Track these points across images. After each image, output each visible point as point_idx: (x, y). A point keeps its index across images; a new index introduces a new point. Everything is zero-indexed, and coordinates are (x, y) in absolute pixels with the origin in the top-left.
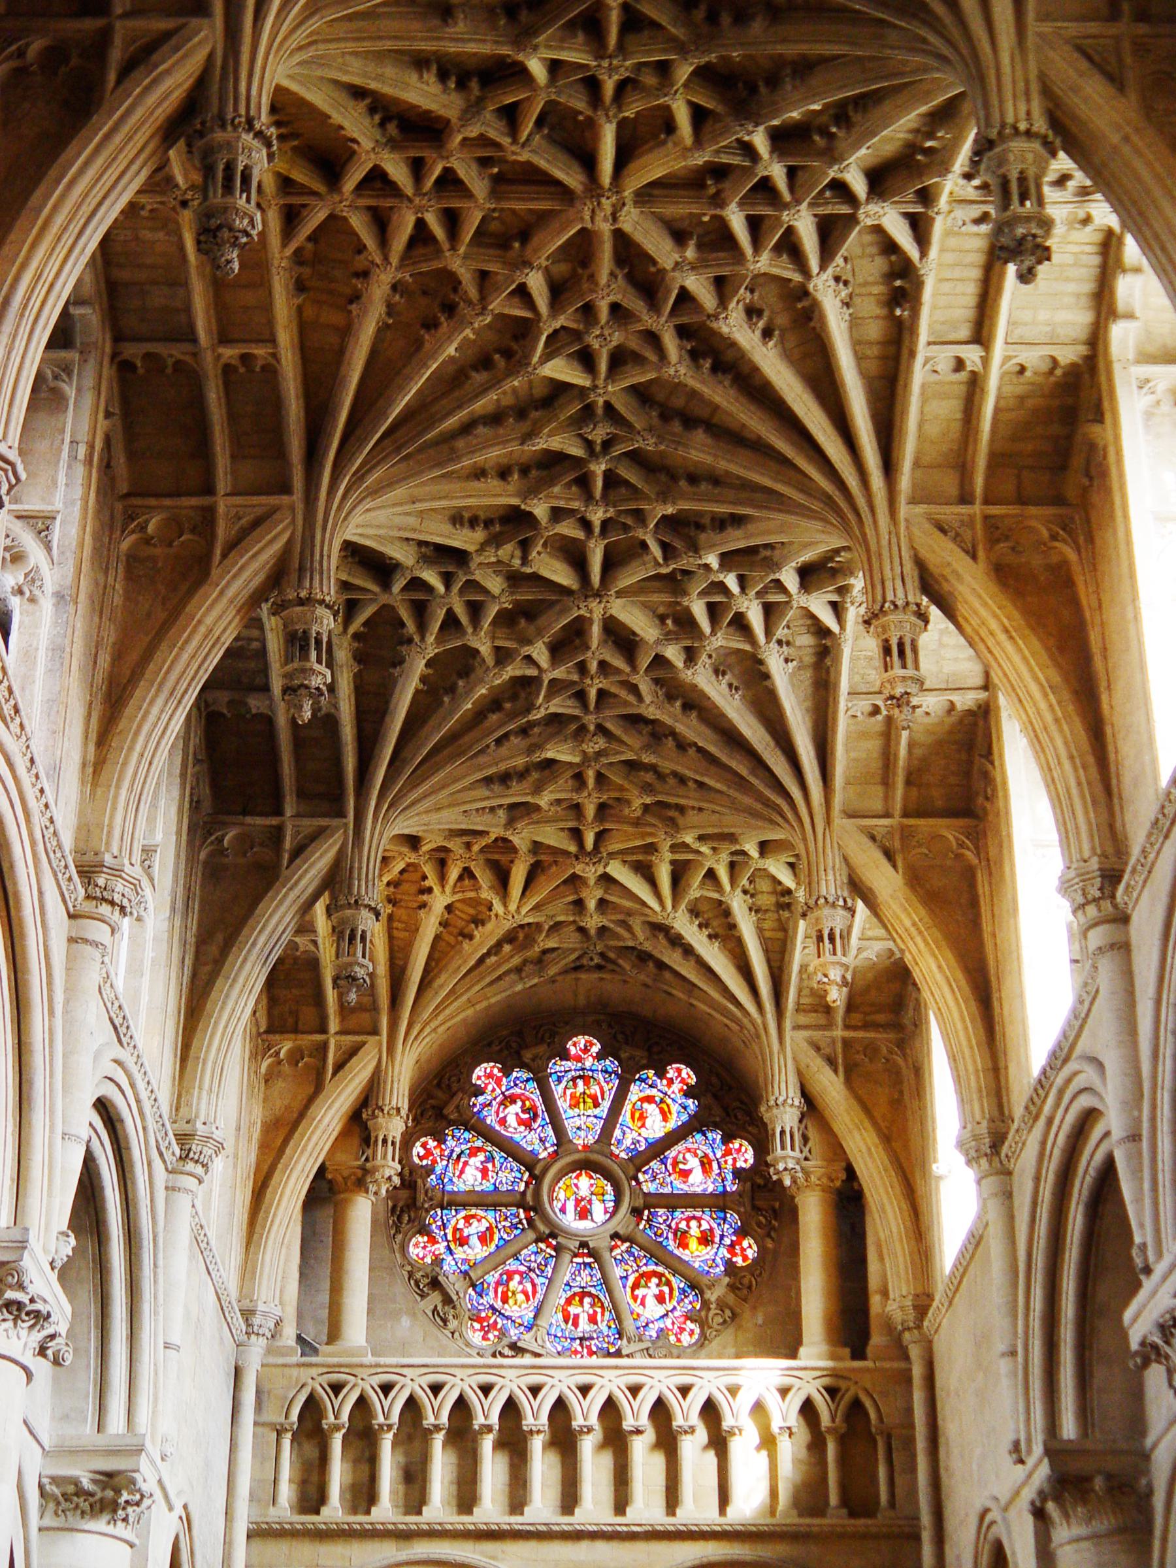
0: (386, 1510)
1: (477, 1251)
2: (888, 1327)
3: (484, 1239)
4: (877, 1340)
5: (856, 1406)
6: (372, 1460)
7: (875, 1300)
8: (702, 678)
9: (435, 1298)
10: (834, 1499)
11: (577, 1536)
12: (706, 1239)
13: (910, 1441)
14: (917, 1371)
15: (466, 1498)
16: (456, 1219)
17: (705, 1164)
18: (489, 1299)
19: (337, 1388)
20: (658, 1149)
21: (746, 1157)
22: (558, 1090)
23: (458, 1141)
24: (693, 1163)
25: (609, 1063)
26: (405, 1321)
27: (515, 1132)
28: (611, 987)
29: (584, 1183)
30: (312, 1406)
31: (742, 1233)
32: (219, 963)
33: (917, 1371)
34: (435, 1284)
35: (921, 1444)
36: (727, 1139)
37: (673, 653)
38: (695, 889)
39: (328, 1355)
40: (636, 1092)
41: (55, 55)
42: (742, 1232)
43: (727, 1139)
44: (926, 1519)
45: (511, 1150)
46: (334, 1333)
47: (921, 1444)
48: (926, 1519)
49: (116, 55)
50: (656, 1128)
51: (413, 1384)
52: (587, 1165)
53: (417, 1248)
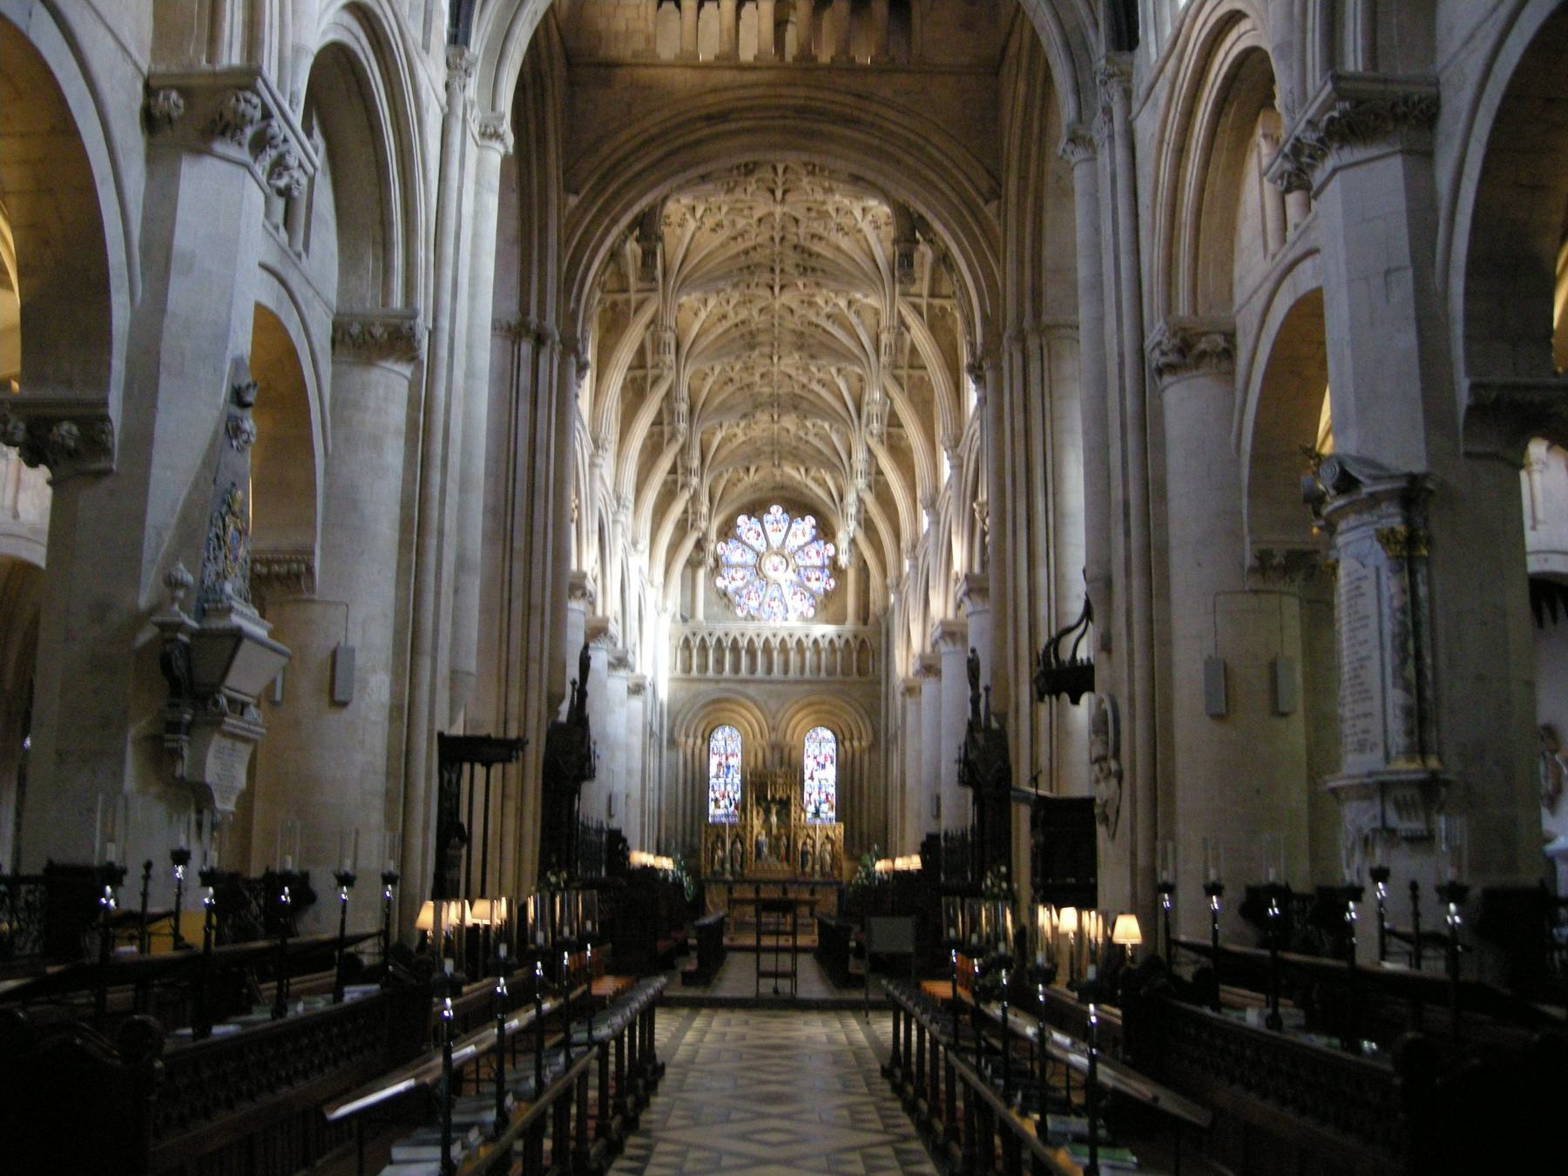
0: (711, 673)
1: (739, 583)
2: (875, 614)
3: (743, 579)
4: (871, 619)
5: (863, 641)
6: (707, 657)
7: (871, 606)
8: (811, 438)
9: (726, 600)
10: (855, 669)
11: (771, 682)
12: (818, 579)
13: (880, 654)
14: (883, 630)
15: (736, 668)
16: (732, 572)
17: (818, 553)
18: (743, 600)
19: (694, 634)
20: (801, 548)
21: (831, 550)
22: (767, 526)
23: (732, 544)
24: (813, 553)
25: (785, 516)
26: (716, 609)
27: (752, 541)
28: (786, 494)
29: (776, 560)
30: (687, 641)
31: (829, 578)
32: (647, 477)
33: (883, 630)
34: (725, 594)
35: (883, 653)
36: (825, 544)
37: (802, 433)
38: (812, 473)
39: (691, 623)
40: (794, 526)
41: (633, 380)
42: (829, 578)
43: (825, 544)
44: (883, 677)
45: (751, 547)
46: (693, 615)
47: (883, 653)
48: (883, 677)
49: (649, 381)
50: (801, 541)
51: (719, 633)
52: (777, 554)
53: (720, 583)
